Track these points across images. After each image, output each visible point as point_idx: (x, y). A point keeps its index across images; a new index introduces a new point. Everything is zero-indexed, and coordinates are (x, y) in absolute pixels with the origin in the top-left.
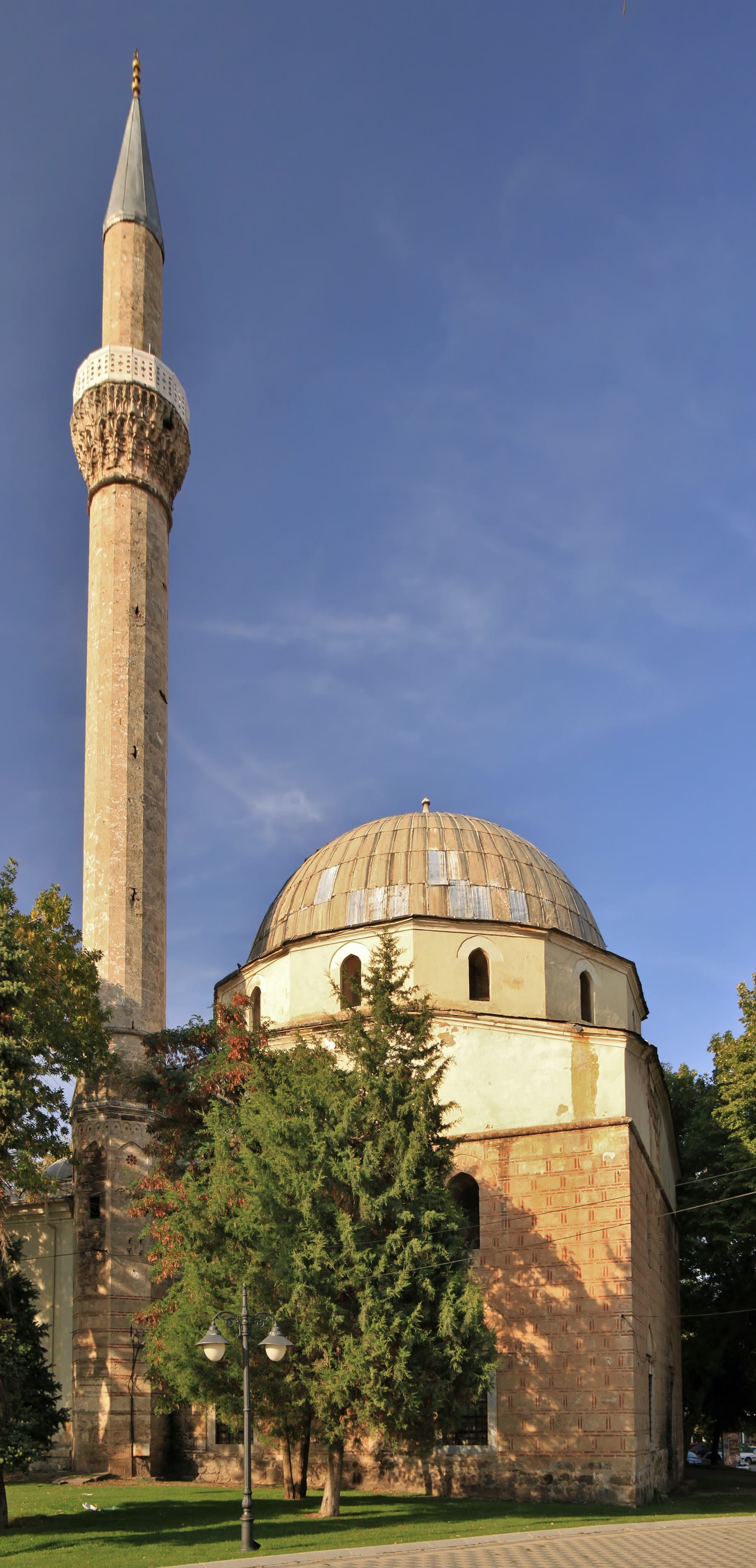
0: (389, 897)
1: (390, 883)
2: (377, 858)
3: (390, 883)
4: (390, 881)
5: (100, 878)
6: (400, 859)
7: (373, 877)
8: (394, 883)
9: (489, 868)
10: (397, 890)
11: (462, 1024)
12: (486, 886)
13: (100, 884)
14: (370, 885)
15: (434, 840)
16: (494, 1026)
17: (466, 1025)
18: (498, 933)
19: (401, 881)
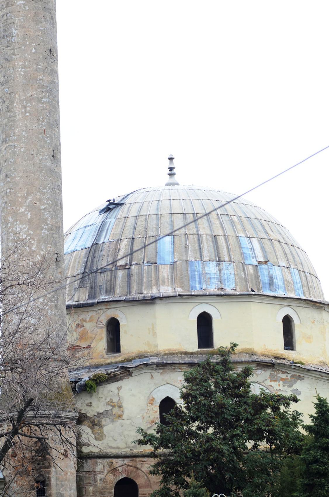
0: (220, 270)
1: (219, 261)
2: (204, 237)
3: (219, 261)
4: (219, 258)
5: (33, 244)
6: (221, 240)
7: (205, 253)
8: (222, 259)
9: (277, 251)
10: (224, 265)
11: (298, 374)
12: (279, 266)
13: (33, 248)
14: (204, 259)
15: (239, 227)
16: (320, 378)
17: (300, 375)
18: (298, 305)
19: (227, 259)
